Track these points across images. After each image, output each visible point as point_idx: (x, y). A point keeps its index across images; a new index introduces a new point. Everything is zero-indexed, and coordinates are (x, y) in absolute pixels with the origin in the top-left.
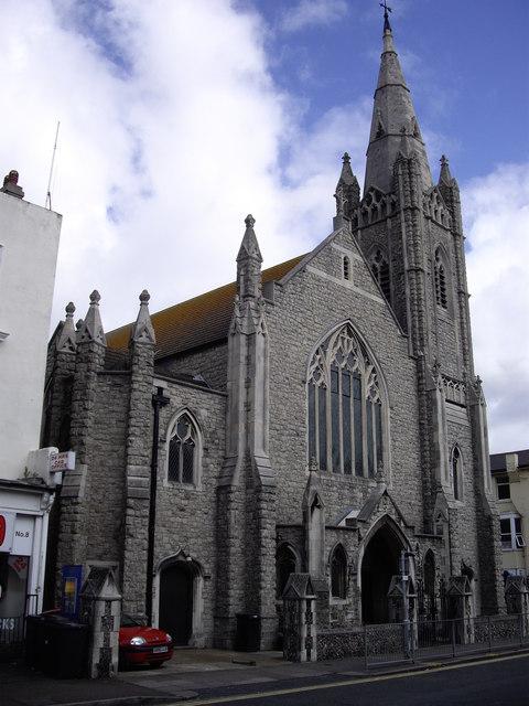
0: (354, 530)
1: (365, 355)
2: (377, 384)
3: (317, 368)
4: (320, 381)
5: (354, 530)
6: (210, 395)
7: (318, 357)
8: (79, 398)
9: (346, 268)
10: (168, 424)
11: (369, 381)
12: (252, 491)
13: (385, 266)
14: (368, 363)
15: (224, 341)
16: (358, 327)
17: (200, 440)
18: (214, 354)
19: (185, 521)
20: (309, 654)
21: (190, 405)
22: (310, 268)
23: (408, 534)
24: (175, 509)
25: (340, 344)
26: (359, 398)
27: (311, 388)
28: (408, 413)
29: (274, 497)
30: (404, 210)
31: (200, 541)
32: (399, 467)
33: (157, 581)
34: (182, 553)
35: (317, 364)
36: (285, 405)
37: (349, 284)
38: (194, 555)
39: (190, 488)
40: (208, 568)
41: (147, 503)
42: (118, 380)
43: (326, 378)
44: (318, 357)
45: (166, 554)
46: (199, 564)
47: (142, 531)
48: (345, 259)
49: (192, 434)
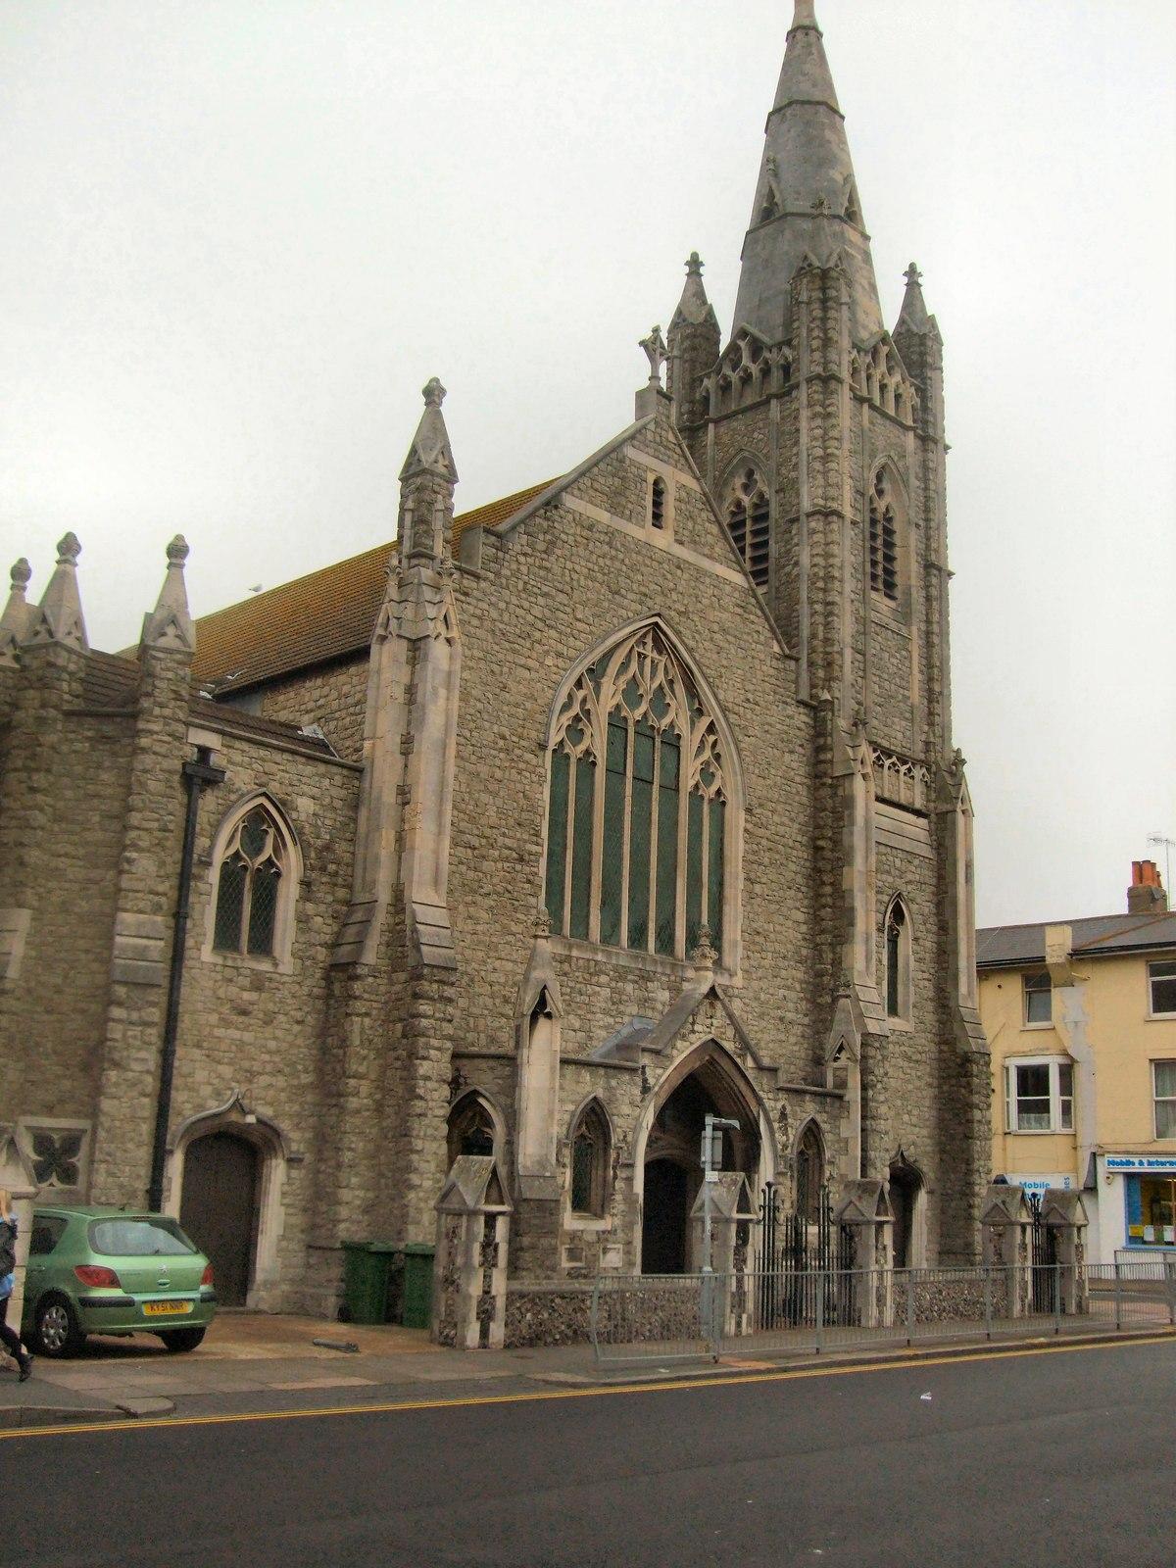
0: (633, 1070)
1: (692, 692)
2: (718, 757)
3: (577, 719)
4: (582, 747)
5: (633, 1070)
6: (322, 768)
7: (581, 694)
9: (657, 504)
10: (216, 826)
11: (701, 749)
12: (402, 976)
13: (762, 502)
14: (700, 712)
15: (361, 655)
16: (678, 633)
17: (292, 864)
18: (343, 680)
19: (248, 1037)
20: (484, 1333)
21: (274, 787)
22: (569, 501)
23: (762, 1085)
24: (226, 1009)
25: (634, 667)
26: (672, 788)
28: (789, 826)
29: (449, 992)
30: (809, 380)
31: (281, 1081)
32: (757, 939)
33: (175, 1166)
34: (238, 1106)
35: (576, 709)
37: (662, 539)
38: (267, 1112)
39: (265, 966)
40: (297, 1140)
41: (160, 996)
42: (108, 729)
43: (597, 739)
44: (581, 694)
45: (201, 1107)
46: (277, 1133)
47: (143, 1054)
48: (656, 483)
49: (276, 850)
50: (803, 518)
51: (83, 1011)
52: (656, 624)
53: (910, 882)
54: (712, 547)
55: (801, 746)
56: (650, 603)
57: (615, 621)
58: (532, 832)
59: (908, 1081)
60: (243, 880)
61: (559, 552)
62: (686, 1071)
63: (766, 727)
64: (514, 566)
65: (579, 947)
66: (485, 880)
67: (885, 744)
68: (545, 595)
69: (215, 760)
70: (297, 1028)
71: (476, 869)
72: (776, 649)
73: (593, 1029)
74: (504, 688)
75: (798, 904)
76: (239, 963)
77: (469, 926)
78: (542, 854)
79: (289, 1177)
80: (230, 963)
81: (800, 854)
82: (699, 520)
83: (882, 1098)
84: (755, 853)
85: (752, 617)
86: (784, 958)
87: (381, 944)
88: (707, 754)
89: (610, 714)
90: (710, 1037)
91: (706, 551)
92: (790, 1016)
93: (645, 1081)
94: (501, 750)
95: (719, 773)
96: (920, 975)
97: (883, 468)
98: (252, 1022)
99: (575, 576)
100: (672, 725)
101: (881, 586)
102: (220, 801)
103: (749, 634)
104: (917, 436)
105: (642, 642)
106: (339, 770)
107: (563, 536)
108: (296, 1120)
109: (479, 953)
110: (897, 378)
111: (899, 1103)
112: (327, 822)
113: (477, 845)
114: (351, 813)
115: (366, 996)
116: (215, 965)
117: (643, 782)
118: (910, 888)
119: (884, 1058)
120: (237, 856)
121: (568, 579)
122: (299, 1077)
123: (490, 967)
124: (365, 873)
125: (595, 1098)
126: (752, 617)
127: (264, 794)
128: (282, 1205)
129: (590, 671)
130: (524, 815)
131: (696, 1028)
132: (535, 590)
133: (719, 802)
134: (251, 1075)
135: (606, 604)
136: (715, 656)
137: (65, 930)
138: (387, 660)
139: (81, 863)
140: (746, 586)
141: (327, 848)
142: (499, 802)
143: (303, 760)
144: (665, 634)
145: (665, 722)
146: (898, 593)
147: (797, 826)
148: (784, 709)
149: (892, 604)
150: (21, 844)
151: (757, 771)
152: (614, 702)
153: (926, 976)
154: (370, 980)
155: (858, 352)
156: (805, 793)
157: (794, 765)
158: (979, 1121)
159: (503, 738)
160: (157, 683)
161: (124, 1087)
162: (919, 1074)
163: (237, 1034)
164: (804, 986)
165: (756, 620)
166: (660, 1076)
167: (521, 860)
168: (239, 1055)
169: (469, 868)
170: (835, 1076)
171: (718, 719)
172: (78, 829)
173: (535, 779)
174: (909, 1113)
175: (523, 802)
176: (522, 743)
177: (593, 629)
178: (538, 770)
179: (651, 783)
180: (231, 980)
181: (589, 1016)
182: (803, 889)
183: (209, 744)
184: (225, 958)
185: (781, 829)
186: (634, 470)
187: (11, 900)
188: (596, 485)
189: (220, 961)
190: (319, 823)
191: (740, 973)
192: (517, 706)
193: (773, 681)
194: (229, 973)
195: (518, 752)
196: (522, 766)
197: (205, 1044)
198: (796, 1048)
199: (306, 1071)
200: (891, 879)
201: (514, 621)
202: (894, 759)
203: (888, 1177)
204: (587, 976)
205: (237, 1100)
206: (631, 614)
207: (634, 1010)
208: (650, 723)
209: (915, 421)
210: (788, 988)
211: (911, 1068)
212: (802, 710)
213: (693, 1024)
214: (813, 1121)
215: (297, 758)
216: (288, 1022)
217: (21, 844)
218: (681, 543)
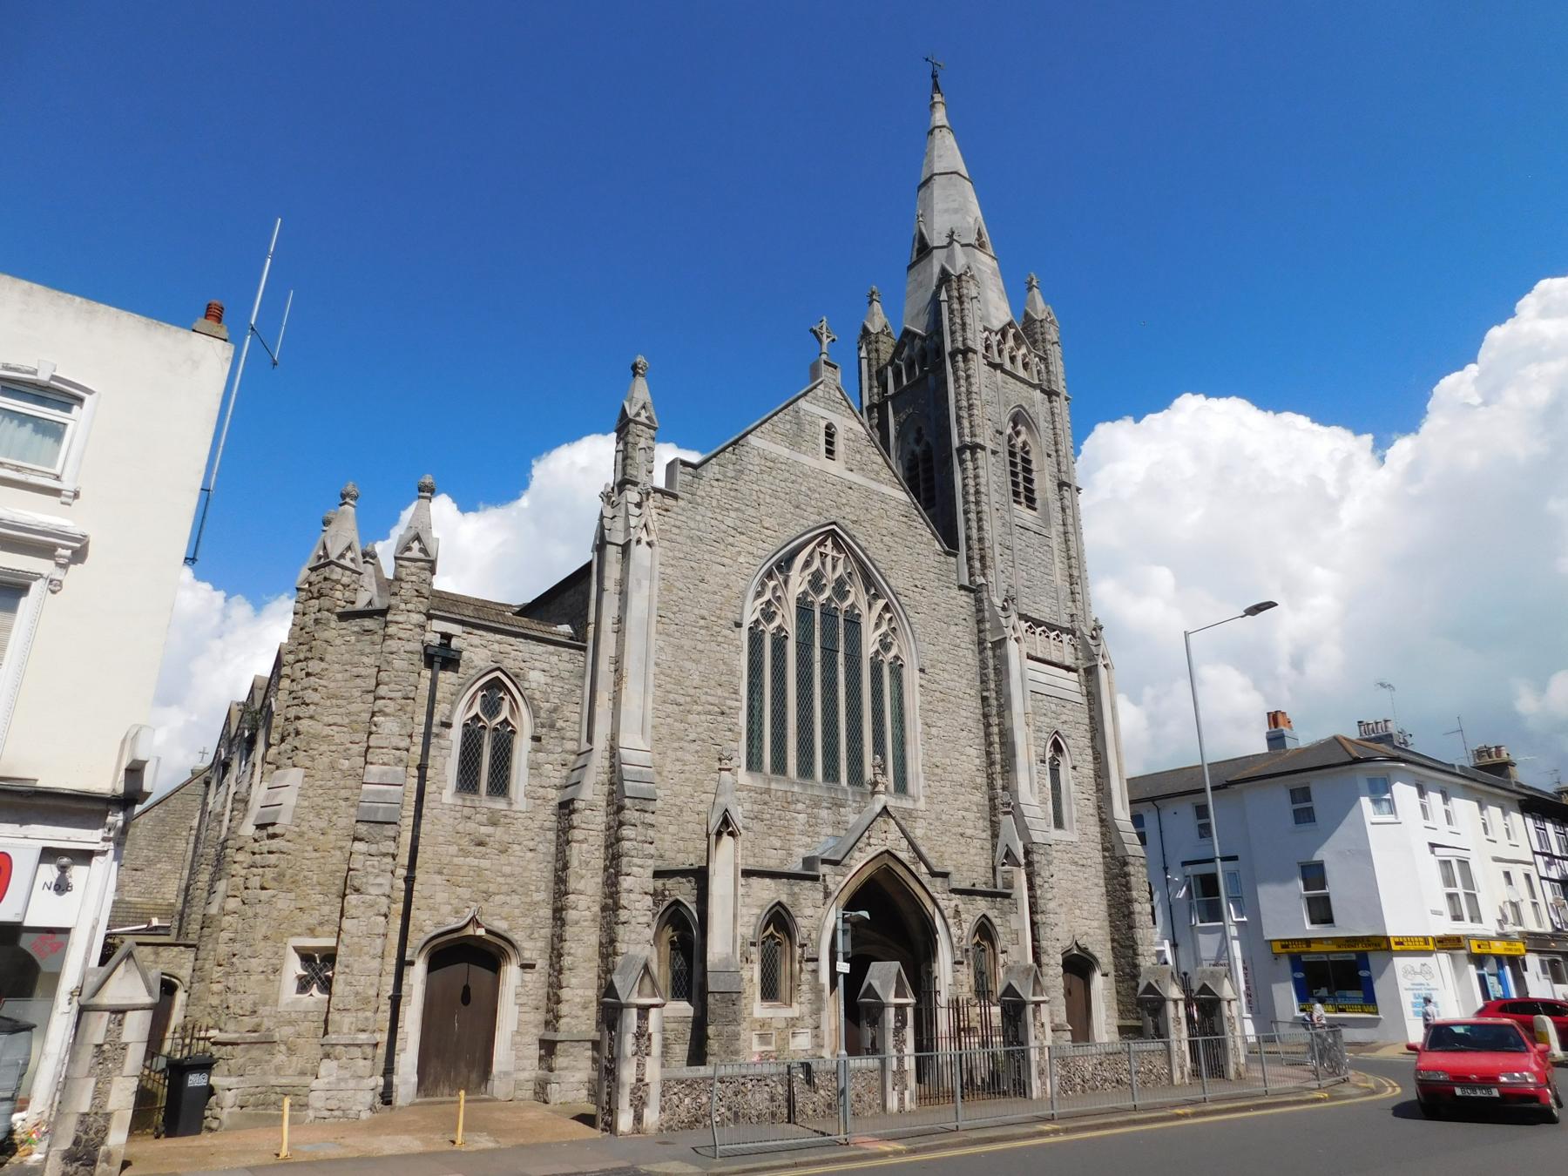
0: (815, 879)
1: (869, 581)
7: (772, 584)
9: (829, 443)
11: (877, 626)
14: (876, 596)
19: (485, 863)
23: (935, 887)
24: (465, 842)
25: (816, 564)
27: (755, 639)
29: (649, 818)
31: (515, 900)
34: (474, 921)
36: (697, 662)
39: (500, 804)
40: (533, 947)
43: (787, 618)
47: (379, 880)
48: (827, 427)
51: (341, 848)
54: (878, 473)
56: (827, 515)
58: (731, 690)
59: (1077, 882)
60: (482, 737)
61: (746, 478)
64: (708, 489)
65: (778, 781)
66: (690, 730)
68: (737, 510)
69: (455, 643)
70: (530, 855)
73: (793, 848)
74: (702, 581)
75: (970, 743)
76: (477, 804)
77: (678, 766)
78: (741, 708)
79: (523, 981)
80: (468, 803)
81: (970, 704)
82: (865, 454)
83: (1049, 896)
88: (884, 628)
89: (798, 599)
92: (969, 832)
93: (826, 887)
94: (701, 627)
96: (1081, 796)
99: (762, 496)
100: (853, 606)
101: (1023, 500)
107: (750, 467)
108: (529, 932)
109: (688, 789)
110: (1023, 350)
111: (1070, 900)
112: (556, 689)
115: (583, 825)
116: (455, 805)
117: (829, 653)
118: (1065, 727)
119: (1050, 863)
120: (476, 718)
121: (755, 498)
122: (532, 896)
123: (697, 800)
128: (516, 1004)
130: (724, 678)
131: (872, 841)
132: (727, 506)
134: (488, 896)
135: (789, 516)
136: (886, 553)
140: (909, 500)
141: (555, 710)
142: (701, 668)
146: (1038, 505)
147: (965, 681)
151: (927, 640)
152: (801, 589)
154: (588, 812)
156: (971, 656)
157: (959, 634)
158: (1139, 913)
160: (403, 585)
161: (362, 909)
162: (1086, 875)
163: (476, 862)
164: (980, 808)
165: (919, 526)
166: (840, 883)
169: (676, 720)
173: (734, 649)
174: (1080, 908)
175: (722, 667)
177: (778, 534)
180: (469, 818)
181: (788, 837)
183: (449, 631)
184: (464, 800)
185: (951, 684)
186: (809, 418)
188: (777, 429)
189: (460, 802)
190: (549, 690)
191: (922, 800)
192: (715, 593)
193: (937, 571)
194: (467, 811)
195: (718, 629)
196: (720, 639)
197: (445, 871)
198: (977, 858)
199: (538, 890)
200: (1048, 720)
201: (710, 529)
203: (1061, 962)
204: (785, 805)
205: (474, 916)
207: (830, 831)
210: (966, 810)
211: (1079, 871)
212: (962, 592)
213: (869, 837)
216: (521, 850)
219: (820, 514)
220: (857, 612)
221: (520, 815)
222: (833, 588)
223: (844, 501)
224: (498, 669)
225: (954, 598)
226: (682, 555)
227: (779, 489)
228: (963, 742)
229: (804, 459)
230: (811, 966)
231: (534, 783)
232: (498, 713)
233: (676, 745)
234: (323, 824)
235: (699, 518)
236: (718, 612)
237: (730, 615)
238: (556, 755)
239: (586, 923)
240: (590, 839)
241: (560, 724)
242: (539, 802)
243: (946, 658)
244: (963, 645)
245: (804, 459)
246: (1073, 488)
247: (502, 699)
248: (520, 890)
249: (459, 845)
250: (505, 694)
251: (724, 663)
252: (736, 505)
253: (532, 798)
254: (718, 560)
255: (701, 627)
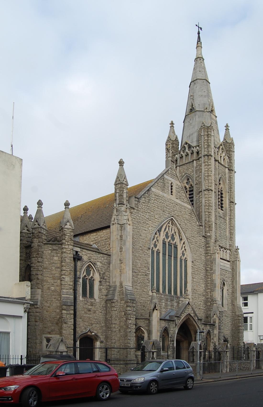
0: (173, 321)
2: (185, 250)
4: (157, 248)
5: (173, 321)
7: (156, 236)
8: (35, 256)
9: (171, 189)
10: (81, 269)
12: (123, 302)
15: (109, 227)
16: (177, 221)
19: (91, 316)
21: (92, 260)
23: (199, 323)
24: (86, 310)
26: (176, 258)
27: (153, 252)
31: (98, 325)
32: (195, 291)
36: (139, 260)
39: (93, 301)
40: (102, 338)
41: (72, 308)
42: (54, 247)
43: (160, 246)
45: (81, 332)
47: (71, 321)
48: (171, 184)
50: (203, 191)
51: (55, 311)
52: (172, 219)
53: (226, 277)
55: (203, 246)
56: (171, 214)
57: (163, 218)
58: (148, 268)
61: (151, 202)
62: (184, 320)
63: (196, 242)
64: (141, 206)
67: (221, 245)
68: (149, 213)
70: (100, 314)
71: (136, 277)
72: (198, 223)
75: (203, 283)
76: (88, 300)
78: (150, 274)
81: (203, 272)
82: (181, 193)
84: (194, 272)
85: (192, 216)
86: (200, 295)
87: (118, 295)
90: (188, 313)
91: (183, 201)
92: (201, 308)
93: (176, 323)
94: (140, 250)
95: (186, 254)
97: (221, 178)
98: (91, 313)
102: (81, 264)
103: (192, 220)
104: (229, 169)
105: (169, 223)
106: (105, 255)
107: (152, 198)
108: (101, 334)
109: (138, 296)
113: (136, 272)
114: (108, 266)
115: (116, 306)
116: (83, 300)
118: (226, 278)
120: (85, 276)
121: (153, 209)
123: (140, 299)
124: (112, 279)
125: (166, 327)
126: (192, 216)
127: (90, 262)
129: (158, 230)
130: (146, 265)
131: (186, 311)
132: (146, 211)
133: (186, 261)
134: (92, 324)
135: (161, 214)
137: (49, 294)
138: (114, 228)
139: (51, 279)
140: (191, 208)
141: (104, 273)
142: (141, 262)
143: (98, 253)
144: (174, 221)
145: (174, 242)
147: (202, 265)
148: (200, 238)
149: (222, 212)
150: (38, 275)
152: (163, 238)
153: (229, 298)
154: (116, 303)
155: (215, 148)
157: (202, 251)
159: (141, 247)
163: (88, 316)
165: (193, 217)
166: (179, 322)
167: (146, 275)
168: (89, 320)
169: (135, 277)
170: (213, 321)
171: (186, 241)
172: (50, 271)
173: (148, 256)
175: (146, 262)
176: (145, 248)
177: (159, 220)
178: (148, 254)
179: (172, 256)
180: (86, 304)
181: (161, 309)
182: (204, 279)
184: (85, 299)
186: (166, 181)
187: (36, 287)
188: (158, 185)
191: (191, 299)
192: (143, 239)
193: (197, 231)
195: (144, 250)
197: (82, 318)
198: (203, 315)
199: (103, 323)
200: (222, 277)
202: (223, 249)
204: (160, 301)
205: (89, 330)
206: (167, 217)
207: (170, 307)
208: (171, 242)
209: (228, 166)
210: (201, 302)
213: (185, 310)
214: (209, 330)
215: (96, 253)
217: (38, 275)
218: (177, 199)
219: (169, 214)
220: (177, 244)
221: (97, 303)
222: (171, 237)
223: (175, 209)
224: (90, 262)
225: (201, 240)
226: (135, 228)
227: (159, 206)
228: (201, 283)
229: (165, 195)
230: (172, 343)
231: (100, 294)
232: (90, 274)
233: (135, 284)
234: (49, 305)
235: (139, 215)
236: (144, 245)
237: (147, 246)
238: (105, 287)
239: (117, 332)
240: (117, 310)
241: (105, 278)
242: (102, 299)
243: (198, 258)
244: (202, 254)
245: (165, 195)
246: (234, 204)
247: (91, 270)
248: (99, 323)
249: (84, 311)
250: (91, 269)
251: (146, 261)
252: (148, 211)
253: (100, 298)
254: (144, 229)
255: (140, 250)
